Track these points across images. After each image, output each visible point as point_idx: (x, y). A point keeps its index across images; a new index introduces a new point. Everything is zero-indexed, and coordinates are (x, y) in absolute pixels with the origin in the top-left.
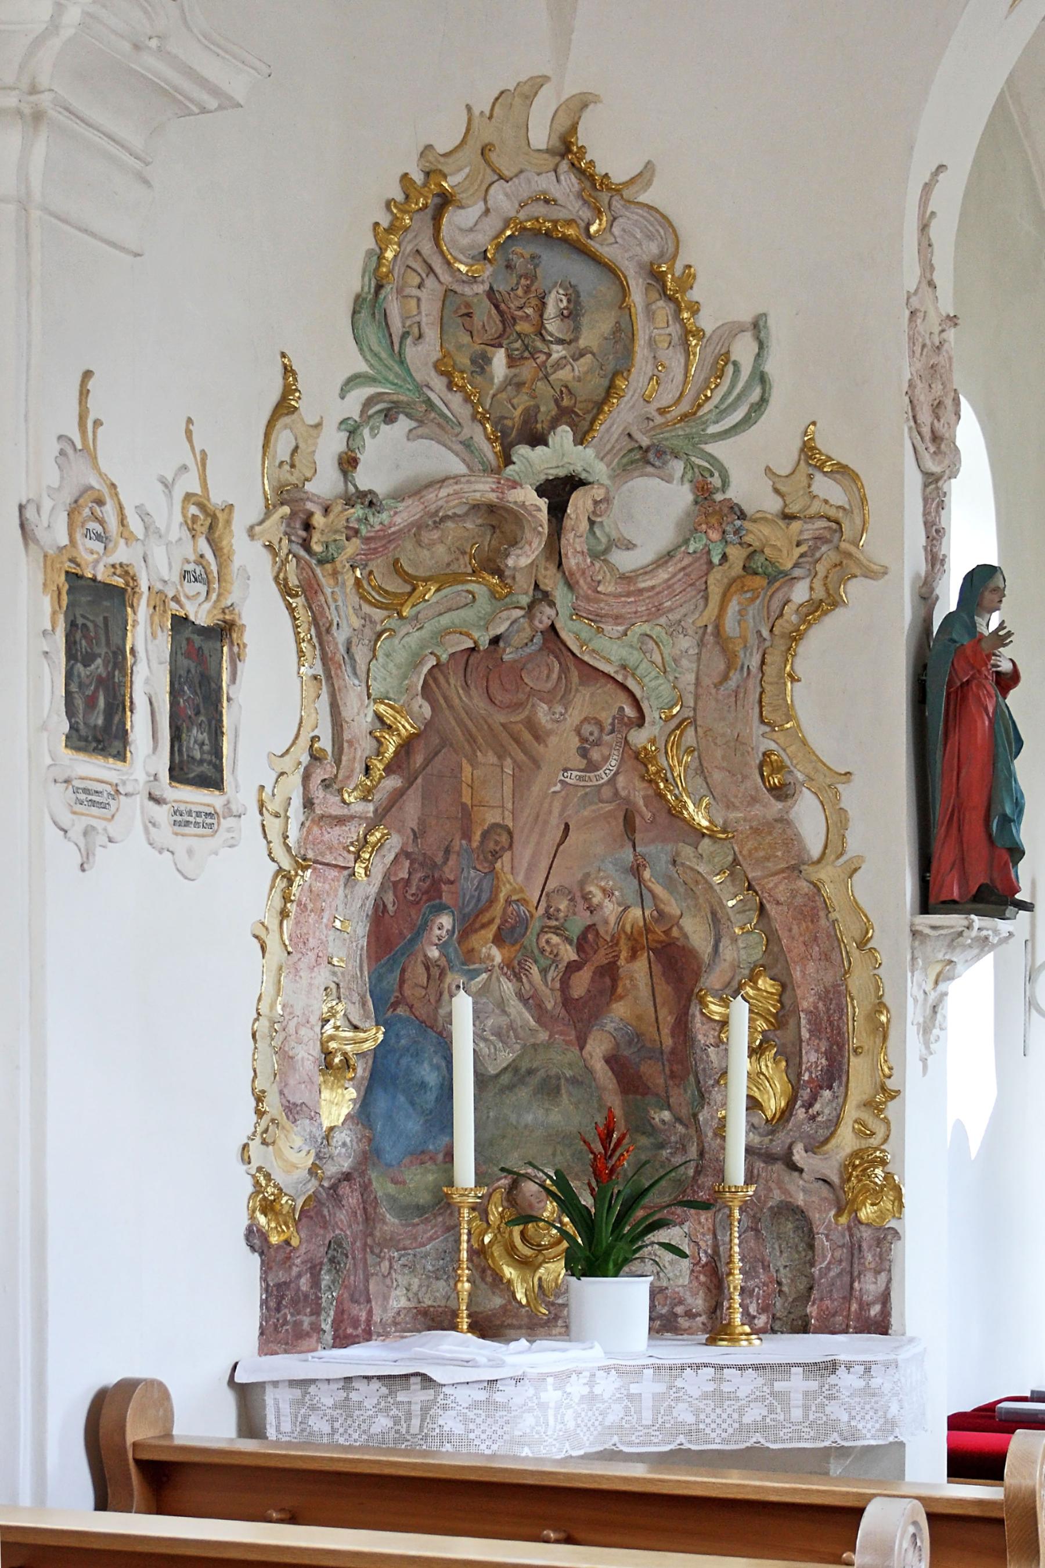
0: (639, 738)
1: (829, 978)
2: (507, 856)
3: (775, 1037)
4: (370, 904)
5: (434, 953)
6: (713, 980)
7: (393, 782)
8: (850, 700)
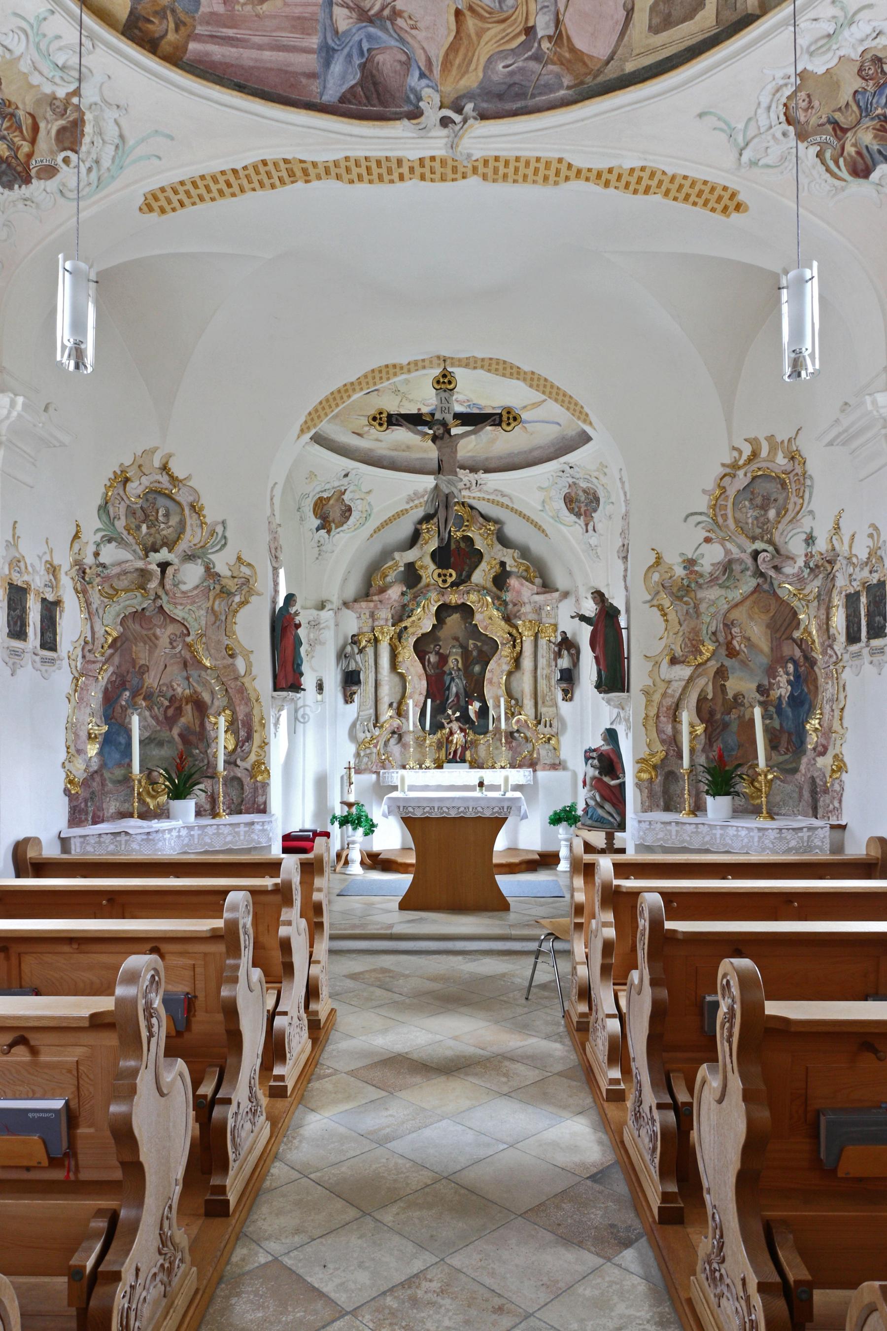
0: (188, 639)
1: (247, 710)
2: (147, 674)
3: (232, 727)
4: (103, 688)
5: (124, 703)
6: (212, 711)
7: (111, 651)
8: (253, 631)
